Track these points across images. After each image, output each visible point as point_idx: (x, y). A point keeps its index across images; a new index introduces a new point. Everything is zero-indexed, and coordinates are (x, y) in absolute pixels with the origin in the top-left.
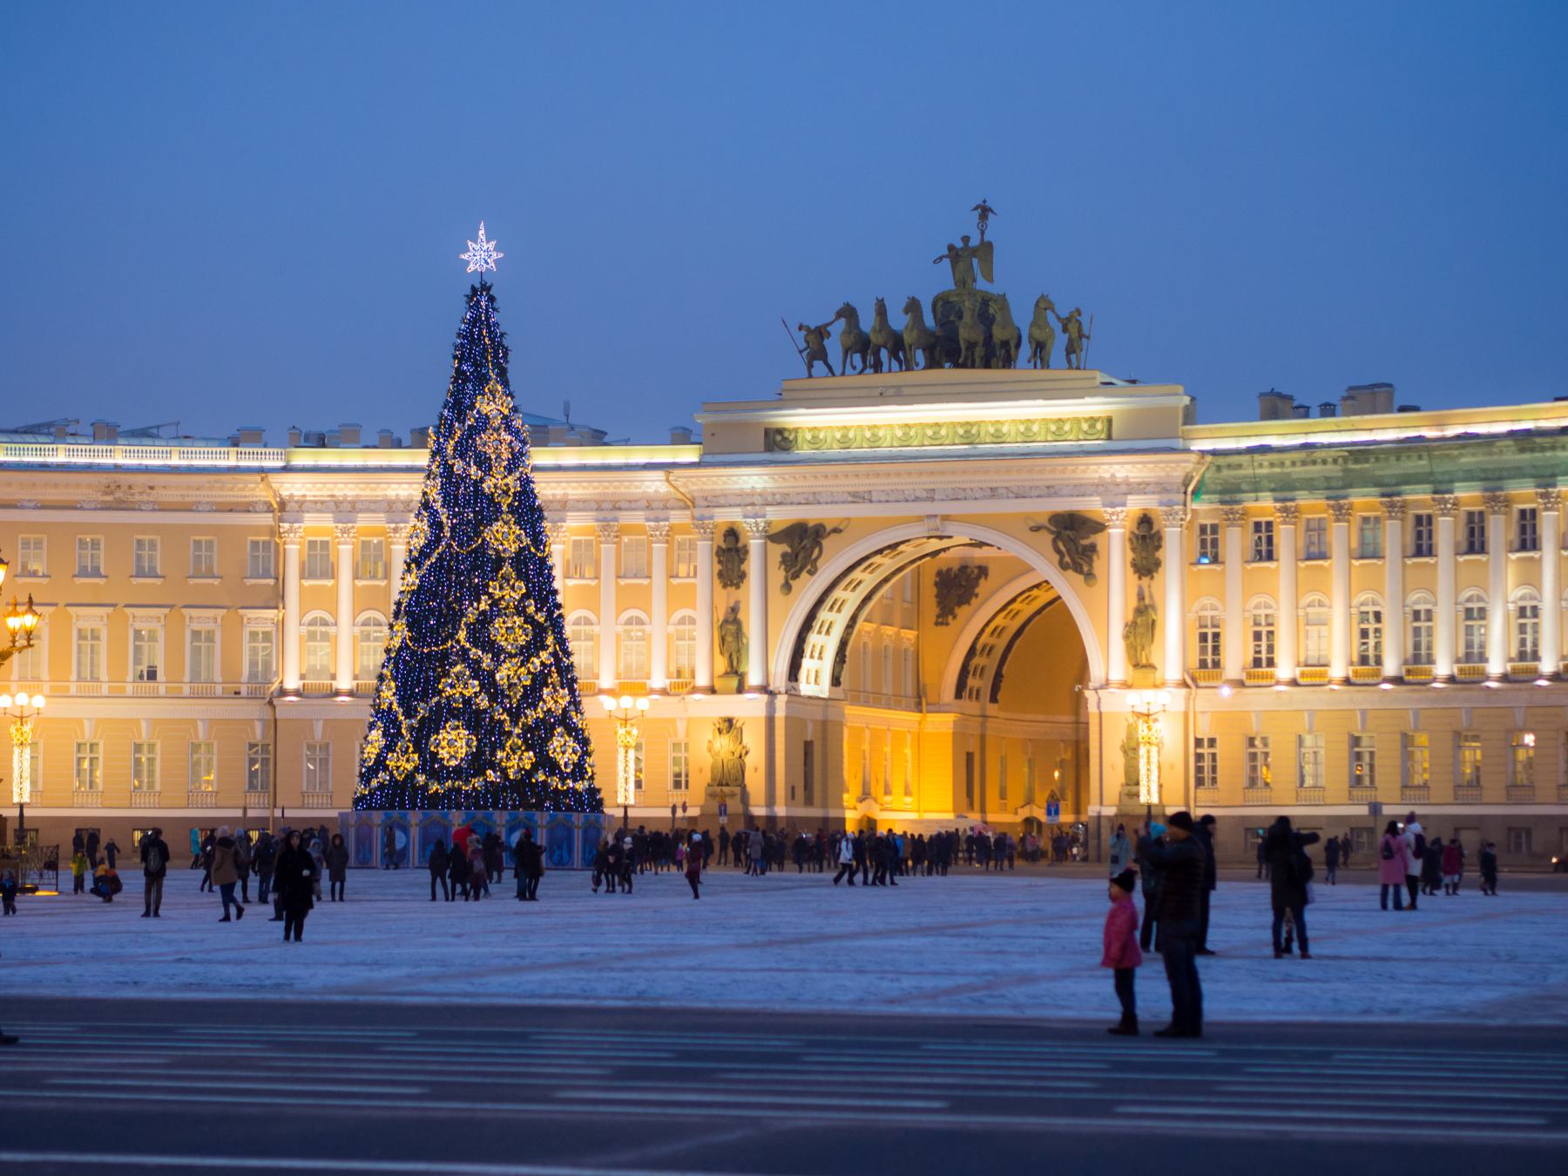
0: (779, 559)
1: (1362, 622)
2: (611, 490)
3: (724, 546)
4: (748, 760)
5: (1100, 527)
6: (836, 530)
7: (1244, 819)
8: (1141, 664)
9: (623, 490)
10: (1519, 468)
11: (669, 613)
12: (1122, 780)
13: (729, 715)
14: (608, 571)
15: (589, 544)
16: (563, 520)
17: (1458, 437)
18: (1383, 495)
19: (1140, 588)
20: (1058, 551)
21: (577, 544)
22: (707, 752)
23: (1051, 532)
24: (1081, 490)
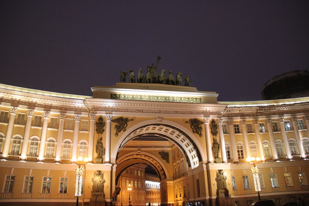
3: (99, 122)
4: (105, 184)
5: (202, 123)
7: (246, 198)
11: (79, 140)
12: (217, 189)
14: (61, 126)
17: (282, 105)
18: (267, 117)
20: (192, 128)
21: (52, 119)
22: (93, 180)
24: (199, 113)
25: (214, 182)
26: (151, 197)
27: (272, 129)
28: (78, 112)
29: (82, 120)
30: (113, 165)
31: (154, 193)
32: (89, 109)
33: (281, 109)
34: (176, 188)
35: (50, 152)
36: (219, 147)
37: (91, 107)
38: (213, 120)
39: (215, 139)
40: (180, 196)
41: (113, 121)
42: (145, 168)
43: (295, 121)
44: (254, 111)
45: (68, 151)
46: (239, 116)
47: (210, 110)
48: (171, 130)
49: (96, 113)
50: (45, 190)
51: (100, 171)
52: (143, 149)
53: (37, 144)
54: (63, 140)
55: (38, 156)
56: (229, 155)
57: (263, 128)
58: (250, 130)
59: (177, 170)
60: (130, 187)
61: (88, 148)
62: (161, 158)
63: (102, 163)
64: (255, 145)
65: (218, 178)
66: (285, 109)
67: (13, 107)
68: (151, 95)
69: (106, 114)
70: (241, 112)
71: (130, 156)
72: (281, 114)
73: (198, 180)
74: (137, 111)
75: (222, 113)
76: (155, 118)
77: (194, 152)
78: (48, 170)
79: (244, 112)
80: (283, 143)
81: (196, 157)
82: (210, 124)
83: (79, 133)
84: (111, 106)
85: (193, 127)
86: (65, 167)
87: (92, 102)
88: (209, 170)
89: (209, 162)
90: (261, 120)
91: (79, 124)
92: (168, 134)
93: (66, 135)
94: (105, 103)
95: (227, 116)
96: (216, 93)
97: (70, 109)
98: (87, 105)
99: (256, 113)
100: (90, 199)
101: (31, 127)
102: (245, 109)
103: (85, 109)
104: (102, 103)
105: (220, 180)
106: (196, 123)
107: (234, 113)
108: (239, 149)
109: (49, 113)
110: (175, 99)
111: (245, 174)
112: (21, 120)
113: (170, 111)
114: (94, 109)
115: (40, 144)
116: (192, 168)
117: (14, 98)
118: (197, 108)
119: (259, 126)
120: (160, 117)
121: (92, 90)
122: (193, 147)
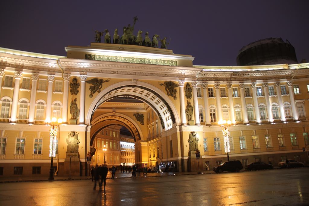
0: (89, 88)
2: (38, 65)
3: (73, 83)
4: (79, 145)
5: (177, 85)
7: (216, 158)
8: (189, 119)
9: (41, 65)
10: (271, 78)
11: (52, 102)
12: (189, 150)
13: (74, 131)
14: (34, 87)
16: (22, 71)
17: (255, 71)
18: (240, 83)
19: (188, 101)
20: (167, 91)
21: (24, 80)
22: (68, 141)
24: (174, 76)
25: (186, 144)
26: (126, 157)
27: (244, 94)
28: (52, 73)
29: (56, 81)
30: (88, 126)
31: (129, 153)
32: (63, 70)
33: (254, 75)
34: (150, 149)
35: (23, 114)
36: (192, 110)
37: (65, 68)
38: (188, 83)
39: (189, 102)
40: (154, 157)
41: (88, 82)
42: (120, 130)
43: (266, 87)
44: (228, 76)
45: (42, 112)
46: (213, 81)
47: (185, 73)
48: (146, 92)
49: (70, 74)
50: (19, 151)
51: (74, 132)
52: (117, 111)
53: (9, 105)
54: (36, 102)
55: (10, 117)
56: (202, 118)
57: (236, 92)
58: (223, 94)
59: (151, 131)
60: (105, 148)
61: (62, 109)
62: (136, 119)
63: (77, 124)
64: (227, 108)
65: (190, 140)
66: (258, 75)
68: (126, 57)
69: (80, 74)
70: (216, 76)
71: (105, 117)
72: (254, 79)
73: (171, 142)
74: (112, 72)
75: (197, 76)
76: (130, 80)
77: (168, 115)
78: (21, 131)
79: (218, 76)
80: (254, 108)
81: (170, 119)
82: (185, 87)
83: (53, 94)
84: (85, 67)
86: (38, 128)
87: (66, 63)
88: (182, 132)
89: (182, 124)
90: (234, 85)
91: (52, 85)
92: (143, 96)
93: (39, 96)
94: (79, 63)
95: (202, 79)
97: (44, 69)
98: (61, 65)
99: (230, 78)
100: (65, 159)
101: (1, 88)
102: (220, 74)
103: (59, 69)
104: (76, 63)
105: (192, 141)
106: (171, 86)
107: (209, 77)
108: (212, 112)
109: (21, 73)
110: (151, 61)
111: (216, 136)
113: (146, 73)
114: (68, 70)
115: (12, 105)
116: (166, 130)
118: (172, 71)
119: (232, 90)
120: (135, 79)
121: (66, 50)
122: (167, 109)
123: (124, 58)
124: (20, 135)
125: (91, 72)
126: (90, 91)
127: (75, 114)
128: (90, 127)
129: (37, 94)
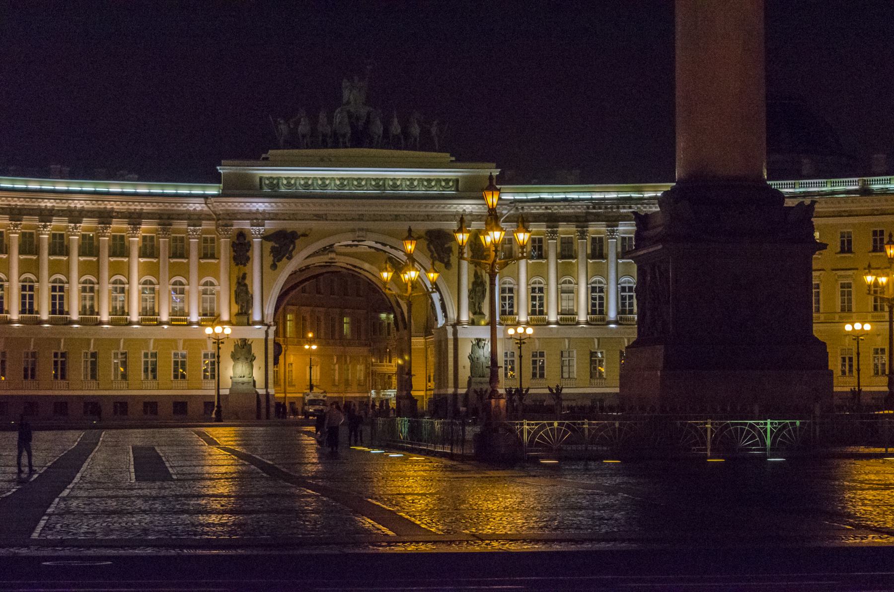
1: (592, 292)
2: (169, 208)
6: (304, 235)
9: (175, 208)
11: (200, 277)
13: (244, 337)
15: (152, 238)
16: (140, 224)
21: (144, 238)
23: (426, 239)
30: (269, 326)
41: (266, 238)
58: (567, 252)
60: (311, 342)
61: (218, 292)
63: (248, 324)
67: (73, 225)
83: (199, 262)
85: (432, 247)
89: (458, 322)
93: (175, 270)
96: (494, 165)
112: (89, 247)
117: (72, 205)
123: (339, 179)
124: (148, 348)
125: (272, 219)
126: (271, 258)
127: (245, 304)
128: (273, 328)
129: (172, 266)
